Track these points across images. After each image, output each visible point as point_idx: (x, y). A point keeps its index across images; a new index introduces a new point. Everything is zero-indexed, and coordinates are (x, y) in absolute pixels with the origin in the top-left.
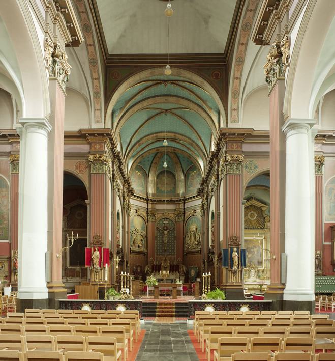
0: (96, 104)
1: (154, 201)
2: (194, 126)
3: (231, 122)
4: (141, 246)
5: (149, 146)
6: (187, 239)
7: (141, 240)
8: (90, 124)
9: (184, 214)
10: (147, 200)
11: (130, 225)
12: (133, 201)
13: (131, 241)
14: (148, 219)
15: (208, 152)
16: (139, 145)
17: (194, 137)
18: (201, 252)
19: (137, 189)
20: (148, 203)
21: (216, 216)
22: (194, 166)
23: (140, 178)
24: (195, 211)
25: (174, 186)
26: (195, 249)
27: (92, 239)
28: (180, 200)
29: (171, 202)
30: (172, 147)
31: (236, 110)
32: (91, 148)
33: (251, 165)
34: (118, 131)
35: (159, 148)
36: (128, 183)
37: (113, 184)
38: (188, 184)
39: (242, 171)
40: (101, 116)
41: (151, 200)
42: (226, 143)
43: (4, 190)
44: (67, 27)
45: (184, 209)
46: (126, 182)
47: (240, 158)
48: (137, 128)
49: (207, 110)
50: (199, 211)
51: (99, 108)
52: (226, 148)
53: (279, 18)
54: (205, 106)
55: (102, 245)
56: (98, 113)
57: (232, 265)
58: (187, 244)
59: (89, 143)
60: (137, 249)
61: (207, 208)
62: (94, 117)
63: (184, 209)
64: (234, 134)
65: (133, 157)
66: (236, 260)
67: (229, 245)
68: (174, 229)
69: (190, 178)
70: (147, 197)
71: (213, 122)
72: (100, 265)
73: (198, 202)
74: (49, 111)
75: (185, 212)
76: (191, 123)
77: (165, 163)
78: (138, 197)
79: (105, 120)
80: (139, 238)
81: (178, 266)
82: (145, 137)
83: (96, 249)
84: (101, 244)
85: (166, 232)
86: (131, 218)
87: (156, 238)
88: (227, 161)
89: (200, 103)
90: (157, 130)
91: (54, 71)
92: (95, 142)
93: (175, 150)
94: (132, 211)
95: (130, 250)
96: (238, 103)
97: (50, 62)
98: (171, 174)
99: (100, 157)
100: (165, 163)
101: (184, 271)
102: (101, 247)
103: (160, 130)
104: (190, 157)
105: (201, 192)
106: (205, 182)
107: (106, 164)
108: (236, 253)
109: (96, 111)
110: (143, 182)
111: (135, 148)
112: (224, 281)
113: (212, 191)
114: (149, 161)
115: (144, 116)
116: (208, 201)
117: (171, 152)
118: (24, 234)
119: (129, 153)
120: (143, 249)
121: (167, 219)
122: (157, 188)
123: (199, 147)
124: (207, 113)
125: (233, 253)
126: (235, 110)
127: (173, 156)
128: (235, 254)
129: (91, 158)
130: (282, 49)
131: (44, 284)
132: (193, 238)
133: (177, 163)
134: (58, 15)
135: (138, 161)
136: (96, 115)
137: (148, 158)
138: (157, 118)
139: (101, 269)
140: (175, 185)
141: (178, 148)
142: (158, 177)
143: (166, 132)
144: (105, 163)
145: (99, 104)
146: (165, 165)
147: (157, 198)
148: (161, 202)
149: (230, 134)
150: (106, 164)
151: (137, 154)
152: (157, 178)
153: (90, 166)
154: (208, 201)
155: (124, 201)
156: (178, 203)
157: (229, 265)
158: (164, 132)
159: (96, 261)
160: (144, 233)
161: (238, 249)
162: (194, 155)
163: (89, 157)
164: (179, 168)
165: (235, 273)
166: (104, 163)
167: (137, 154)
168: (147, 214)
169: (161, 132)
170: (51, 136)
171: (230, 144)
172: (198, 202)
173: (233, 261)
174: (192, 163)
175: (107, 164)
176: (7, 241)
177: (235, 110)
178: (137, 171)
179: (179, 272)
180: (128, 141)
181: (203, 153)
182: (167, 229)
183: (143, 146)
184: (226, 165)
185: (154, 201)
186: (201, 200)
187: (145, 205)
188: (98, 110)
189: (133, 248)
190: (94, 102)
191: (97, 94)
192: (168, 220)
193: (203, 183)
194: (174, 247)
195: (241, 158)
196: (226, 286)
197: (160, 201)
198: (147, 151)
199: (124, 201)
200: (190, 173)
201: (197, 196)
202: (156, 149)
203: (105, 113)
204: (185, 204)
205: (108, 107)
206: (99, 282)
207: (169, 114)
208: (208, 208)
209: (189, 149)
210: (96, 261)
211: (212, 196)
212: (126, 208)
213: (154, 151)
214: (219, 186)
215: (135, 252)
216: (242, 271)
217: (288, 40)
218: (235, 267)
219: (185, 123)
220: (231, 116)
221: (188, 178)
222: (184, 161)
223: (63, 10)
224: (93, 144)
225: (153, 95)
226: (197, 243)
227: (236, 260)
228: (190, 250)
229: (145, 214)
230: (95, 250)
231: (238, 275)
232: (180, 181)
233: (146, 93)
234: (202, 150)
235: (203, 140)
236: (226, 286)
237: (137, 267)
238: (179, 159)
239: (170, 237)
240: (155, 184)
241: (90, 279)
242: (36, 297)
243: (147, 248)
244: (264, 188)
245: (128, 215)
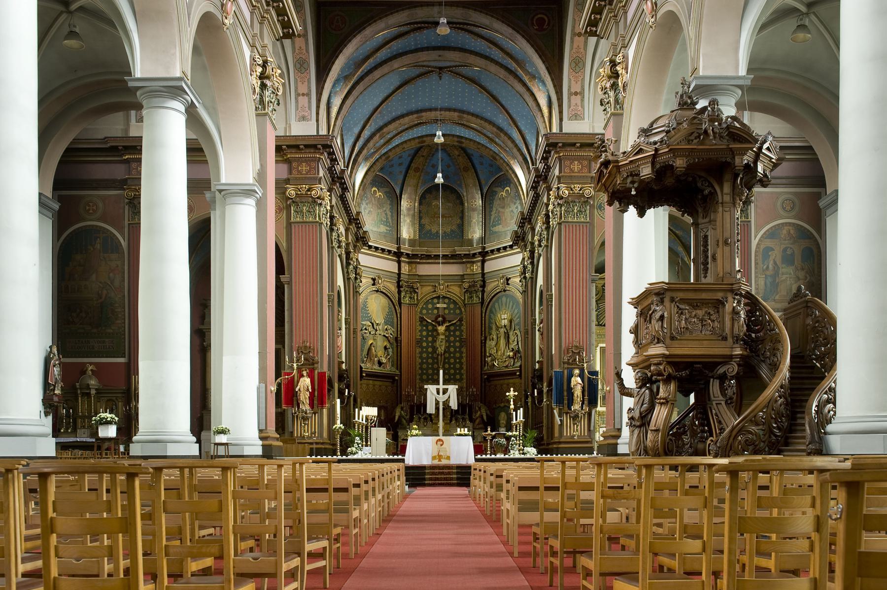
0: (300, 84)
1: (413, 258)
3: (570, 119)
4: (384, 360)
5: (403, 134)
6: (491, 344)
7: (385, 348)
8: (288, 125)
9: (483, 286)
10: (398, 254)
13: (362, 351)
14: (400, 299)
15: (533, 154)
17: (502, 120)
18: (520, 376)
19: (375, 229)
20: (399, 262)
21: (545, 299)
22: (506, 179)
23: (380, 205)
24: (508, 280)
25: (459, 221)
26: (507, 367)
28: (474, 254)
30: (453, 136)
31: (580, 94)
32: (290, 172)
34: (339, 122)
35: (425, 139)
36: (356, 224)
37: (331, 235)
38: (492, 217)
39: (592, 216)
40: (310, 108)
41: (407, 254)
44: (278, 20)
45: (483, 274)
46: (354, 221)
47: (587, 191)
48: (376, 103)
49: (526, 79)
50: (516, 280)
51: (305, 92)
52: (560, 172)
53: (616, 16)
54: (520, 72)
55: (316, 365)
56: (303, 100)
57: (571, 402)
58: (491, 355)
60: (376, 368)
61: (532, 278)
62: (297, 109)
63: (483, 274)
64: (574, 145)
65: (366, 159)
66: (578, 392)
67: (564, 363)
68: (461, 320)
69: (496, 203)
70: (399, 248)
71: (538, 105)
72: (312, 405)
73: (515, 259)
74: (258, 167)
75: (484, 281)
76: (495, 93)
77: (440, 175)
78: (377, 248)
81: (471, 407)
83: (305, 373)
84: (313, 364)
85: (441, 329)
87: (419, 342)
88: (562, 198)
89: (513, 65)
90: (420, 105)
91: (262, 101)
92: (300, 161)
94: (365, 281)
95: (361, 372)
96: (583, 80)
97: (258, 90)
98: (452, 192)
99: (308, 190)
100: (440, 175)
101: (482, 416)
103: (427, 105)
104: (495, 159)
105: (519, 239)
106: (526, 220)
107: (321, 204)
108: (579, 380)
109: (300, 98)
110: (389, 214)
111: (371, 144)
112: (556, 434)
113: (540, 246)
114: (400, 164)
117: (453, 146)
118: (225, 359)
120: (388, 369)
121: (444, 297)
123: (513, 142)
124: (525, 85)
125: (573, 379)
126: (576, 94)
127: (457, 153)
128: (576, 381)
130: (618, 68)
131: (256, 434)
132: (502, 342)
133: (466, 169)
134: (267, 11)
135: (379, 165)
136: (300, 106)
137: (400, 157)
138: (419, 82)
139: (315, 413)
140: (462, 218)
141: (466, 139)
143: (441, 109)
144: (319, 201)
145: (306, 83)
146: (439, 179)
147: (421, 250)
149: (565, 145)
150: (321, 204)
151: (375, 153)
152: (420, 204)
153: (288, 208)
154: (532, 263)
156: (468, 262)
157: (566, 402)
158: (436, 109)
159: (304, 397)
162: (503, 155)
163: (286, 189)
164: (471, 180)
165: (575, 418)
166: (316, 202)
167: (375, 153)
168: (399, 287)
169: (430, 110)
170: (261, 205)
171: (567, 163)
172: (515, 259)
173: (573, 394)
175: (324, 203)
177: (576, 94)
178: (374, 189)
179: (471, 420)
180: (356, 131)
184: (559, 204)
185: (415, 256)
186: (520, 256)
187: (390, 266)
188: (303, 95)
191: (301, 65)
192: (446, 301)
193: (524, 223)
194: (461, 363)
196: (560, 443)
197: (429, 257)
198: (397, 146)
199: (348, 264)
200: (496, 192)
201: (511, 247)
202: (417, 141)
203: (319, 100)
204: (486, 264)
205: (323, 88)
206: (311, 438)
207: (446, 76)
208: (534, 279)
209: (491, 140)
210: (304, 397)
211: (540, 255)
212: (353, 274)
213: (415, 145)
214: (549, 240)
215: (372, 375)
216: (590, 415)
217: (625, 57)
218: (576, 407)
219: (481, 92)
220: (569, 106)
221: (491, 203)
222: (482, 164)
223: (275, 4)
224: (294, 164)
226: (511, 354)
227: (578, 392)
228: (496, 370)
230: (302, 376)
231: (584, 422)
232: (474, 210)
233: (396, 46)
234: (519, 150)
235: (523, 129)
236: (560, 443)
238: (471, 161)
239: (452, 339)
240: (417, 217)
241: (292, 433)
242: (247, 451)
245: (357, 293)
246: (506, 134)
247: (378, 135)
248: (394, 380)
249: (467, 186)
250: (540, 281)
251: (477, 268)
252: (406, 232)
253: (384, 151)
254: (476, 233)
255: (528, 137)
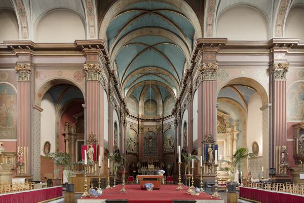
1: (143, 120)
2: (171, 61)
9: (163, 128)
10: (138, 119)
11: (126, 135)
12: (128, 119)
16: (132, 76)
17: (171, 69)
22: (169, 95)
27: (88, 137)
29: (154, 120)
33: (223, 73)
40: (95, 32)
42: (202, 55)
43: (12, 96)
50: (173, 126)
56: (92, 29)
59: (85, 55)
60: (131, 151)
69: (167, 103)
79: (99, 33)
80: (133, 144)
82: (136, 70)
83: (91, 146)
85: (151, 140)
86: (127, 131)
93: (156, 83)
94: (128, 126)
98: (154, 102)
102: (96, 144)
103: (146, 65)
105: (174, 112)
115: (135, 53)
116: (180, 116)
119: (125, 80)
122: (145, 111)
126: (210, 25)
129: (86, 67)
135: (132, 90)
138: (144, 54)
142: (145, 103)
147: (145, 117)
148: (147, 120)
153: (85, 76)
155: (121, 116)
160: (136, 141)
161: (213, 145)
168: (138, 128)
174: (168, 93)
176: (15, 140)
177: (210, 25)
180: (123, 72)
181: (177, 81)
182: (150, 139)
183: (135, 78)
185: (143, 119)
186: (174, 118)
187: (137, 122)
188: (92, 26)
189: (129, 151)
190: (88, 19)
195: (216, 66)
199: (121, 116)
203: (99, 30)
204: (164, 122)
213: (142, 84)
220: (207, 31)
225: (140, 26)
229: (137, 129)
230: (90, 147)
234: (176, 79)
235: (177, 71)
237: (132, 163)
243: (138, 151)
244: (228, 100)
245: (125, 128)
246: (172, 74)
247: (130, 75)
248: (137, 155)
249: (158, 99)
250: (185, 118)
251: (161, 123)
252: (141, 113)
253: (133, 85)
254: (160, 113)
255: (179, 74)
